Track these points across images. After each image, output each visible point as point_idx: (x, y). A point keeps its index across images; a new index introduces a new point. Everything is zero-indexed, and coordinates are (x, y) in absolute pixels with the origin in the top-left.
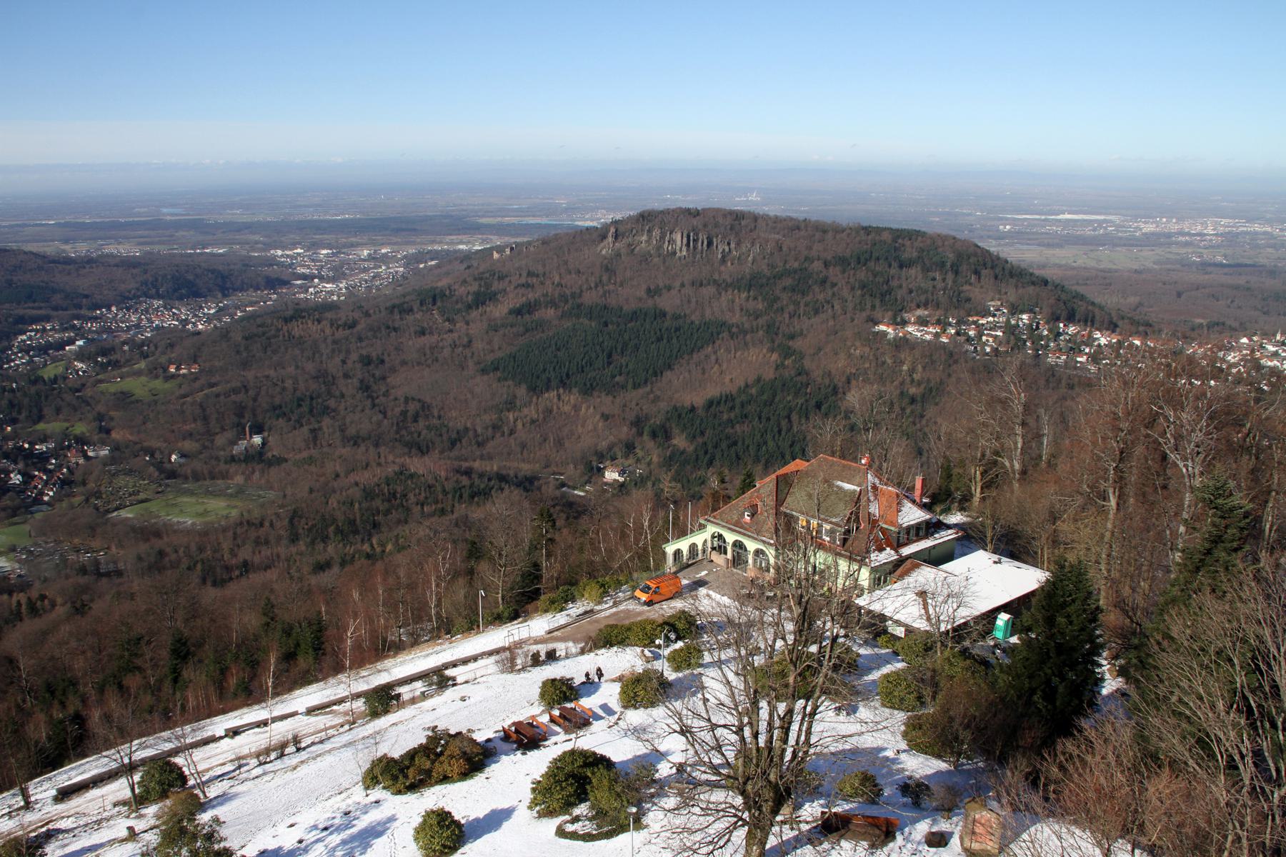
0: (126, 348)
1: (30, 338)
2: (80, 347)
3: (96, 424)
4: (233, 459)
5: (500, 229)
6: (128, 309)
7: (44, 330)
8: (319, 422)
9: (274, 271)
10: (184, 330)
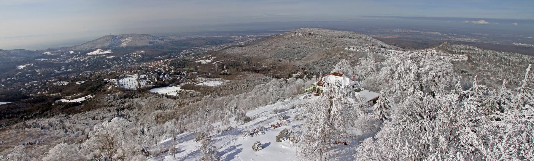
0: (202, 54)
1: (184, 53)
3: (195, 68)
4: (221, 74)
5: (274, 32)
7: (186, 51)
9: (231, 40)
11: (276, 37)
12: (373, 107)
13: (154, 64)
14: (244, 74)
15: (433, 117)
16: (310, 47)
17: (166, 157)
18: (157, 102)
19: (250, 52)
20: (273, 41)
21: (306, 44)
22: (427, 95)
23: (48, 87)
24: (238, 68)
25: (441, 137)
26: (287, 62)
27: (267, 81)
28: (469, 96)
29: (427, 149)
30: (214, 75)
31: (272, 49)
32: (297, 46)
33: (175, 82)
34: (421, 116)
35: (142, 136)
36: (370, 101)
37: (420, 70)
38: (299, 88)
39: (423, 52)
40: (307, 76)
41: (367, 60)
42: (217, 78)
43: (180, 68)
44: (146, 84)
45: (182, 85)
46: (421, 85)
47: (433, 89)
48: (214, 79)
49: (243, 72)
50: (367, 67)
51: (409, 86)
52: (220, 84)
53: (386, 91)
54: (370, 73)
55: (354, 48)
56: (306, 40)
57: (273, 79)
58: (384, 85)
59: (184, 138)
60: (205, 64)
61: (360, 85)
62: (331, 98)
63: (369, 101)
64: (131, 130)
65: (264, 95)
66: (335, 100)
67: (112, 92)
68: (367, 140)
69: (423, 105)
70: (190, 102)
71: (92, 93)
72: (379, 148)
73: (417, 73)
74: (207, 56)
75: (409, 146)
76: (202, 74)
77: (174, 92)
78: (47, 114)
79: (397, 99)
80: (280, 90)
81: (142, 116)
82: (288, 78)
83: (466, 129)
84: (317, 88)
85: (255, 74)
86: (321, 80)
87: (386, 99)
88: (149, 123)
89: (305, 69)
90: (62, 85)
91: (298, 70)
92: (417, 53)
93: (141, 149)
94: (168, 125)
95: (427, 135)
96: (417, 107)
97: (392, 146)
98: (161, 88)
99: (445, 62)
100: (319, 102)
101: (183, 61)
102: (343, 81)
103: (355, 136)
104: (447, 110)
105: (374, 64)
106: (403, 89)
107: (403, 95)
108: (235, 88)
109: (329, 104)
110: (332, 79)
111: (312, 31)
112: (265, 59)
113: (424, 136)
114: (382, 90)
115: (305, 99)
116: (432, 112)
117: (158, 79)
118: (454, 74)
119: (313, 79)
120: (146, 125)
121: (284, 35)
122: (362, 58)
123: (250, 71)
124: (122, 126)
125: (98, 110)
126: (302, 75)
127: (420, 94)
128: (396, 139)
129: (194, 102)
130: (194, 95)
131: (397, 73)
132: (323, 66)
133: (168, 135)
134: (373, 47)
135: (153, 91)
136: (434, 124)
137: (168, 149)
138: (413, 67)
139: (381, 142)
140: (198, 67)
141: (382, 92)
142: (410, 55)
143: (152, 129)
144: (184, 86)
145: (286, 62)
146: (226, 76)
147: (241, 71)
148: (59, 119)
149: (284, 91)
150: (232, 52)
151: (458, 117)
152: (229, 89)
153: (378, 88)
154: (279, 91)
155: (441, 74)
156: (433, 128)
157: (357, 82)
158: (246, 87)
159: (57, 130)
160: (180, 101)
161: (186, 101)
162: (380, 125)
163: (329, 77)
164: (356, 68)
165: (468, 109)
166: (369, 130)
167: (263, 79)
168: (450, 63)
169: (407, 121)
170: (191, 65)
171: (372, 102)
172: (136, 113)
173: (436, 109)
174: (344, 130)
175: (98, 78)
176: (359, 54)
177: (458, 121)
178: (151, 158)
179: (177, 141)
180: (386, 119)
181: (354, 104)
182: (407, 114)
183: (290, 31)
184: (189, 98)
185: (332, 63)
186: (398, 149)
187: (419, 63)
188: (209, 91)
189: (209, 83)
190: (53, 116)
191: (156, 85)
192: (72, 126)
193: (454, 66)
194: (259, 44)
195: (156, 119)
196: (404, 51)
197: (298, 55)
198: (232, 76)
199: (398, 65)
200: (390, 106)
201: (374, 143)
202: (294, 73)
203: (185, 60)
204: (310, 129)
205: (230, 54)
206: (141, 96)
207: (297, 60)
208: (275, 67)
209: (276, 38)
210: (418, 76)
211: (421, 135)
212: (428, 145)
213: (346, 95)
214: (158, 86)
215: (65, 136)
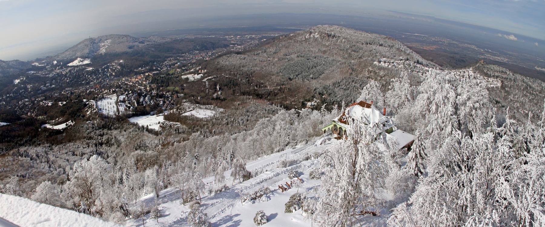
0: (189, 65)
2: (179, 65)
3: (181, 87)
4: (213, 99)
6: (190, 54)
8: (235, 88)
10: (203, 60)
11: (284, 39)
12: (407, 157)
13: (134, 80)
14: (243, 100)
15: (470, 167)
16: (330, 57)
17: (148, 221)
18: (137, 138)
19: (251, 64)
20: (281, 45)
21: (325, 52)
22: (465, 136)
23: (36, 108)
24: (235, 90)
25: (478, 194)
26: (298, 81)
27: (274, 112)
28: (503, 134)
29: (465, 212)
30: (204, 100)
31: (279, 59)
32: (313, 55)
33: (157, 108)
34: (460, 167)
35: (121, 185)
36: (404, 147)
37: (458, 99)
38: (315, 126)
39: (460, 73)
40: (326, 106)
41: (401, 82)
42: (208, 105)
43: (163, 87)
44: (126, 110)
45: (166, 114)
46: (459, 121)
47: (470, 126)
48: (204, 107)
49: (242, 97)
50: (401, 94)
51: (447, 123)
52: (212, 115)
53: (422, 131)
54: (403, 103)
55: (385, 62)
56: (325, 45)
57: (280, 110)
58: (420, 122)
59: (169, 196)
60: (193, 81)
61: (392, 123)
62: (356, 143)
63: (402, 147)
64: (109, 175)
65: (269, 137)
66: (361, 147)
67: (91, 119)
68: (400, 207)
69: (461, 151)
70: (175, 142)
71: (72, 119)
72: (414, 217)
73: (455, 103)
74: (195, 69)
75: (447, 210)
76: (190, 97)
77: (156, 124)
78: (35, 142)
79: (434, 142)
80: (290, 129)
81: (121, 158)
82: (301, 110)
83: (500, 178)
84: (338, 127)
85: (257, 101)
86: (344, 115)
87: (423, 143)
88: (129, 168)
89: (323, 95)
90: (47, 105)
91: (314, 96)
92: (455, 74)
93: (120, 204)
94: (149, 174)
95: (465, 192)
96: (455, 154)
97: (429, 213)
98: (141, 117)
99: (482, 89)
100: (341, 150)
101: (167, 75)
102: (371, 116)
103: (386, 202)
104: (484, 155)
105: (409, 89)
106: (440, 127)
107: (440, 137)
108: (232, 123)
109: (354, 153)
110: (357, 111)
111: (332, 31)
112: (270, 75)
113: (462, 194)
114: (418, 131)
115: (323, 145)
116: (470, 160)
117: (138, 102)
118: (490, 105)
119: (333, 111)
120: (125, 170)
121: (295, 36)
122: (394, 79)
123: (251, 95)
124: (100, 169)
125: (78, 143)
126: (319, 105)
127: (458, 134)
128: (433, 203)
129: (179, 142)
130: (180, 131)
131: (434, 104)
132: (346, 90)
133: (150, 189)
134: (408, 61)
135: (133, 120)
136: (472, 177)
137: (150, 209)
138: (450, 94)
139: (415, 208)
140: (185, 85)
141: (417, 133)
142: (447, 77)
143: (131, 178)
144: (168, 115)
145: (299, 82)
146: (219, 101)
147: (239, 95)
148: (44, 149)
149: (296, 130)
150: (227, 63)
151: (494, 165)
152: (223, 125)
153: (413, 127)
154: (289, 131)
155: (477, 105)
156: (471, 182)
157: (389, 117)
158: (245, 122)
159: (43, 164)
160: (164, 138)
161: (171, 139)
162: (415, 183)
163: (354, 108)
164: (389, 94)
165: (502, 153)
166: (402, 192)
167: (267, 109)
168: (486, 90)
169: (445, 175)
170: (176, 83)
171: (406, 149)
172: (114, 151)
173: (474, 154)
174: (372, 193)
175: (77, 98)
176: (391, 72)
177: (493, 170)
178: (130, 219)
179: (160, 200)
180: (422, 173)
181: (384, 153)
182: (445, 165)
183: (304, 29)
184: (174, 134)
185: (358, 85)
186: (434, 217)
187: (457, 89)
188: (198, 126)
189: (198, 112)
190: (39, 145)
191: (136, 112)
192: (55, 161)
193: (490, 94)
194: (262, 49)
195: (136, 164)
196: (442, 69)
197: (314, 69)
198: (227, 103)
199: (435, 90)
200: (426, 155)
201: (408, 210)
202: (309, 101)
203: (169, 74)
204: (330, 193)
205: (225, 66)
206: (119, 127)
207: (312, 78)
208: (283, 90)
209: (284, 41)
210: (456, 108)
211: (459, 193)
212: (466, 206)
213: (376, 139)
214: (138, 113)
215: (48, 173)
